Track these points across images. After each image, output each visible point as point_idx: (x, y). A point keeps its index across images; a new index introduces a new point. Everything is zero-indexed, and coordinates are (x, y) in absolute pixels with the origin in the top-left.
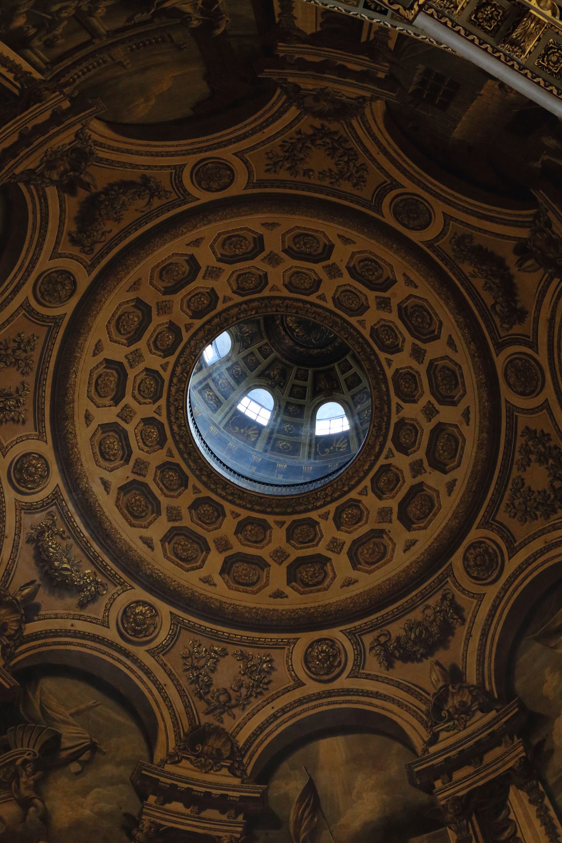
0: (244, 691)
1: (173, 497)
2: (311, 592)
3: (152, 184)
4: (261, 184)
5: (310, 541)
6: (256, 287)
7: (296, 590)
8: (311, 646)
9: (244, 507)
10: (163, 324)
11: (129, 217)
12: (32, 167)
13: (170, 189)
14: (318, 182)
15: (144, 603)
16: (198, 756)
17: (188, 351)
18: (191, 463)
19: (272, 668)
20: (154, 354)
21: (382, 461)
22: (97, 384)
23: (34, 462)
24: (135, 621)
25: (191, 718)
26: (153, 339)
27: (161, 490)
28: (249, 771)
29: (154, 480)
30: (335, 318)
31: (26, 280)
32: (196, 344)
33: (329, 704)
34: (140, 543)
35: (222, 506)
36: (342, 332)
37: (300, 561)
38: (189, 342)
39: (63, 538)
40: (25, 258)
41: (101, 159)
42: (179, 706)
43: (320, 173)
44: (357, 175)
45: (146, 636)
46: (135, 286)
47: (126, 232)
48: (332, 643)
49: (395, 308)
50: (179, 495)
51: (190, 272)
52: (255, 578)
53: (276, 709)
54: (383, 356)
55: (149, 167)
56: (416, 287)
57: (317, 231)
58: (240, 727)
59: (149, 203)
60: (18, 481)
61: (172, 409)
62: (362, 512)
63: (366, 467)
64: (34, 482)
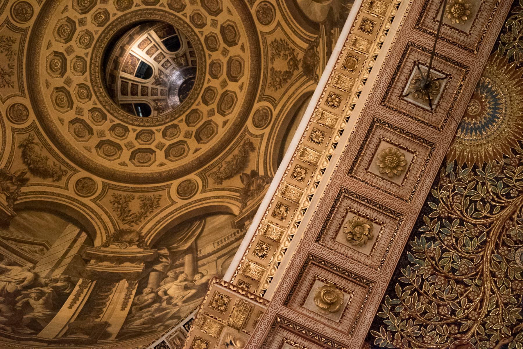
0: (287, 52)
1: (203, 115)
2: (238, 30)
3: (24, 143)
4: (22, 90)
5: (215, 39)
6: (86, 89)
7: (239, 39)
8: (261, 23)
9: (204, 77)
10: (111, 134)
11: (45, 153)
12: (5, 197)
13: (28, 134)
14: (16, 61)
15: (253, 118)
16: (315, 66)
17: (125, 120)
18: (185, 110)
19: (275, 40)
20: (127, 137)
21: (167, 9)
22: (143, 163)
23: (182, 188)
24: (261, 120)
25: (301, 76)
26: (119, 138)
27: (199, 122)
28: (316, 36)
29: (194, 126)
30: (97, 47)
31: (79, 201)
32: (122, 116)
33: (283, 4)
34: (225, 127)
35: (206, 89)
36: (104, 42)
37: (226, 41)
38: (121, 120)
39: (222, 166)
40: (65, 201)
41: (5, 166)
42: (297, 84)
43: (10, 60)
44: (7, 41)
45: (268, 113)
46: (88, 149)
47: (55, 155)
48: (258, 11)
49: (83, 16)
50: (201, 112)
51: (80, 123)
52: (237, 63)
53: (291, 32)
54: (112, 19)
55: (13, 144)
56: (67, 6)
57: (47, 61)
58: (301, 48)
59: (36, 144)
60: (190, 194)
61: (157, 124)
62: (195, 14)
63: (173, 16)
64: (192, 186)
